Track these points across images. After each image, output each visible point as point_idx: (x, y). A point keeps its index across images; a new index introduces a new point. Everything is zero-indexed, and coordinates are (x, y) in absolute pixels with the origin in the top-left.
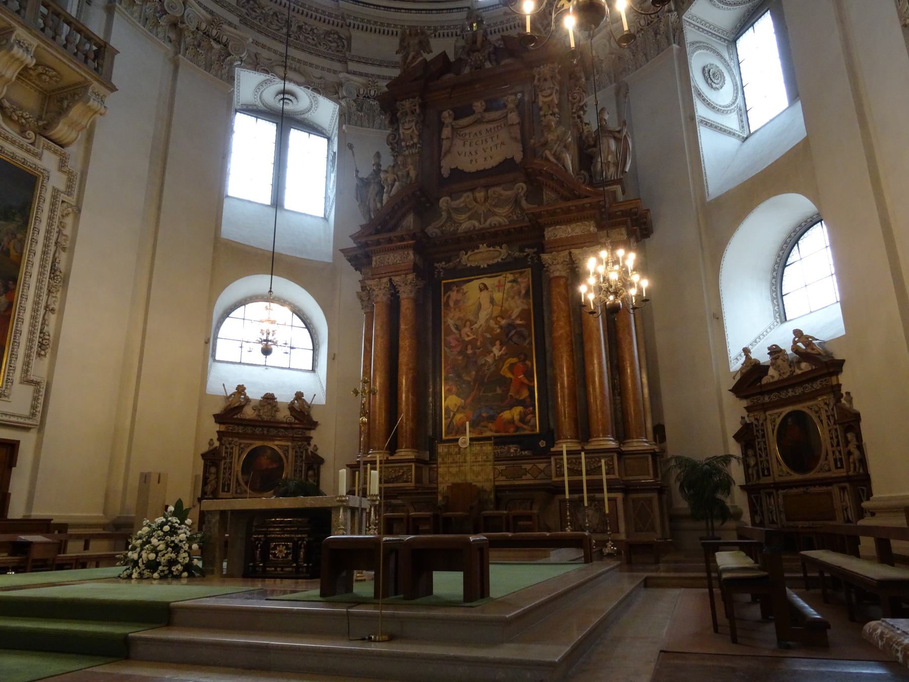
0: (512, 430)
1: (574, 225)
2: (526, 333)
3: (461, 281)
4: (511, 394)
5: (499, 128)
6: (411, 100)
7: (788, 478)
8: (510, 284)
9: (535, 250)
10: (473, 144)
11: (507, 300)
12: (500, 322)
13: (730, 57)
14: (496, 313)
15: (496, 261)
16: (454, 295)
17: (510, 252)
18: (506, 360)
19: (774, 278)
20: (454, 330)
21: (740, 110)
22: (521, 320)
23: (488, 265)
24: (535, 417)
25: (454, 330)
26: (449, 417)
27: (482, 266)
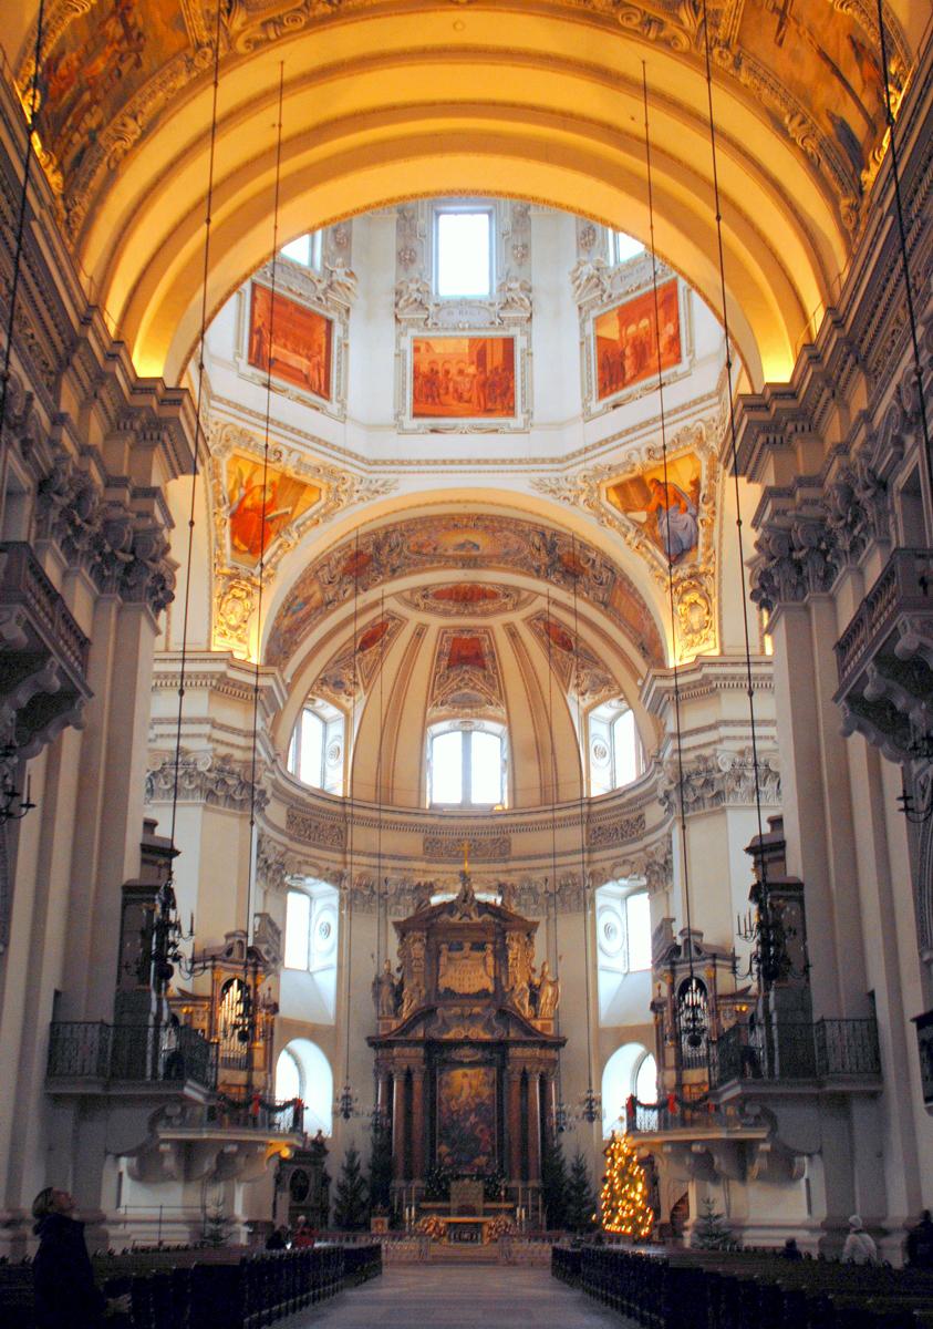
16: (445, 1078)
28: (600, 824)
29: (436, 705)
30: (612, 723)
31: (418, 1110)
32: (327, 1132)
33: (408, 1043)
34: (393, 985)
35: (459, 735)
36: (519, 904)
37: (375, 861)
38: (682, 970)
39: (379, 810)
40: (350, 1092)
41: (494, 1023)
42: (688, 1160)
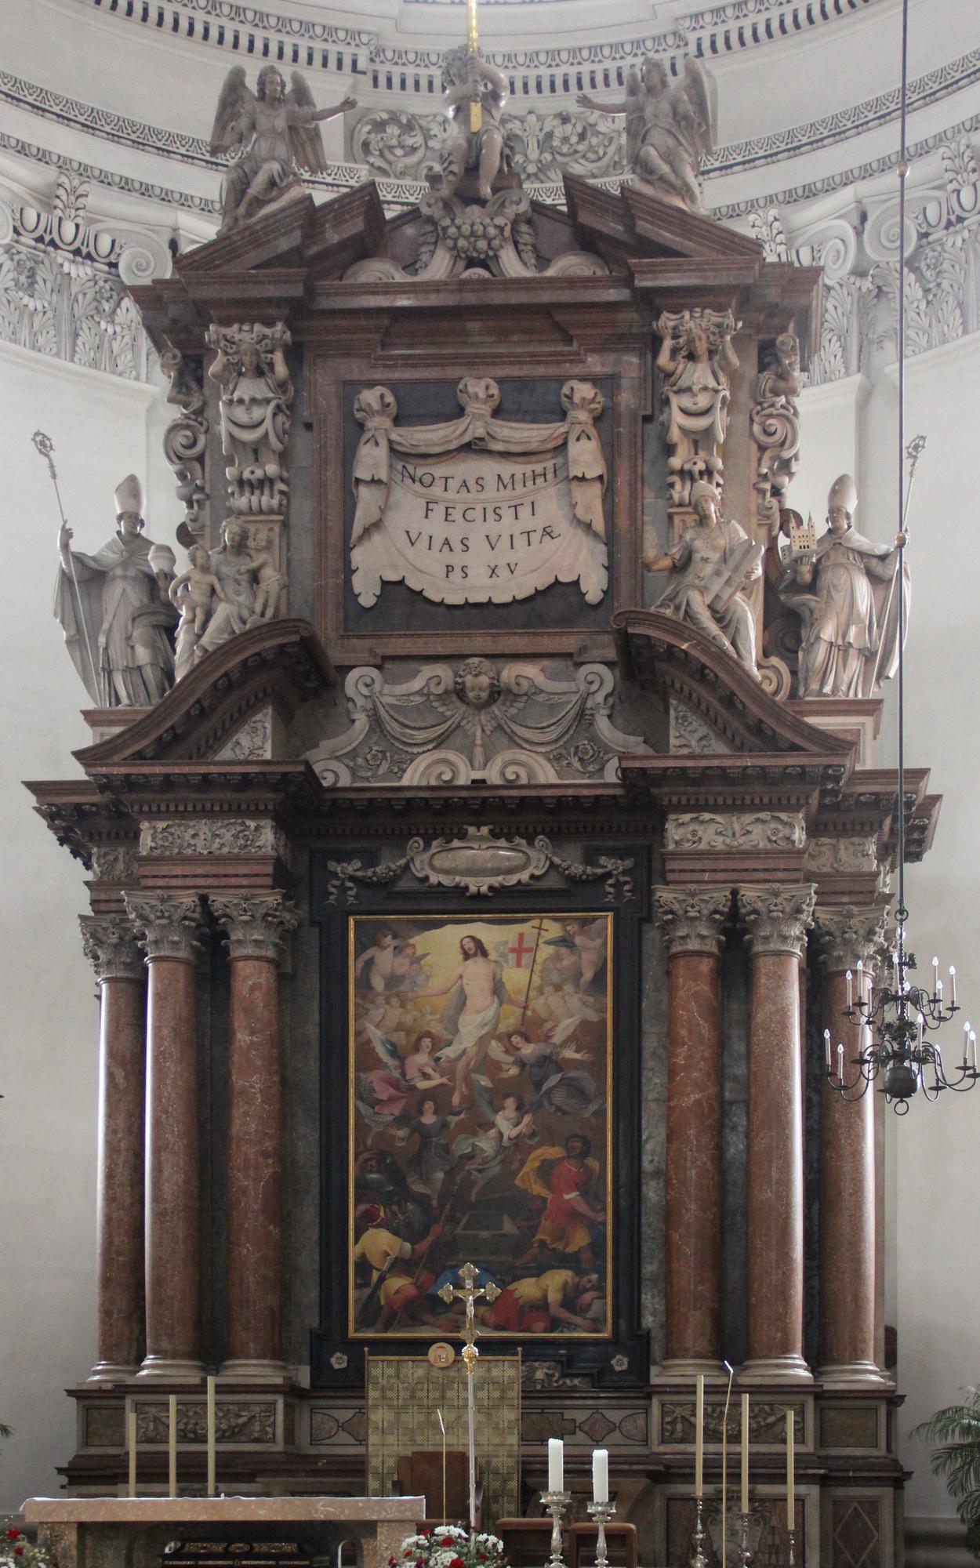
0: (541, 1325)
2: (590, 1086)
3: (408, 921)
4: (543, 1237)
5: (540, 480)
8: (551, 949)
9: (629, 863)
10: (456, 514)
11: (541, 992)
12: (519, 1049)
14: (510, 1022)
15: (512, 880)
17: (557, 860)
18: (533, 1148)
20: (385, 1057)
22: (577, 1051)
23: (491, 888)
24: (605, 1297)
25: (385, 1057)
26: (368, 1285)
27: (473, 889)
41: (603, 725)
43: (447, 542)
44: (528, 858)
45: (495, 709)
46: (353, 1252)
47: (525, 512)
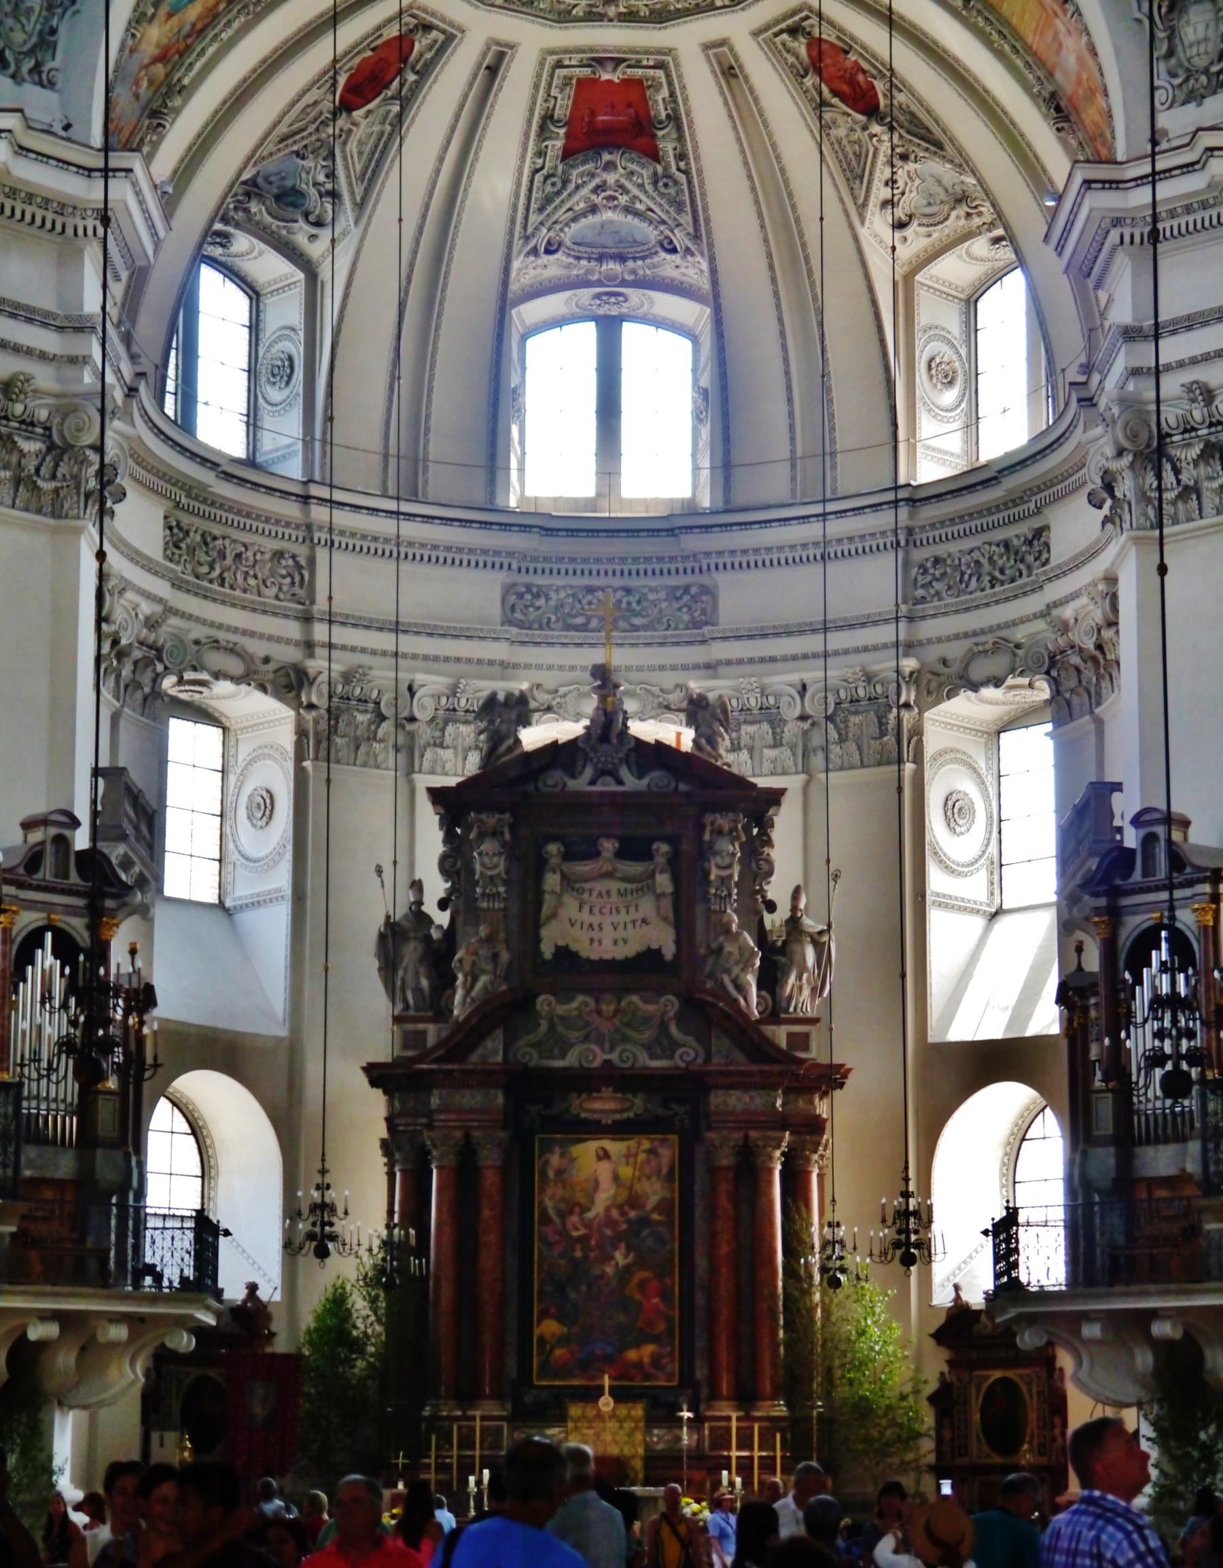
1: (753, 1093)
6: (497, 816)
7: (989, 1461)
10: (596, 910)
11: (639, 1179)
13: (987, 764)
14: (623, 1196)
15: (625, 1115)
16: (555, 1160)
17: (649, 1106)
19: (1006, 1154)
20: (555, 1218)
21: (992, 863)
22: (660, 1214)
24: (672, 1362)
27: (604, 1121)
28: (940, 550)
29: (534, 252)
30: (970, 303)
31: (490, 1238)
32: (270, 1292)
33: (469, 1079)
34: (428, 937)
35: (587, 333)
36: (735, 748)
37: (385, 641)
38: (1136, 909)
39: (397, 514)
40: (331, 1195)
41: (674, 1030)
42: (1144, 1360)
43: (591, 926)
44: (633, 1104)
45: (617, 1022)
46: (537, 1332)
47: (632, 910)
